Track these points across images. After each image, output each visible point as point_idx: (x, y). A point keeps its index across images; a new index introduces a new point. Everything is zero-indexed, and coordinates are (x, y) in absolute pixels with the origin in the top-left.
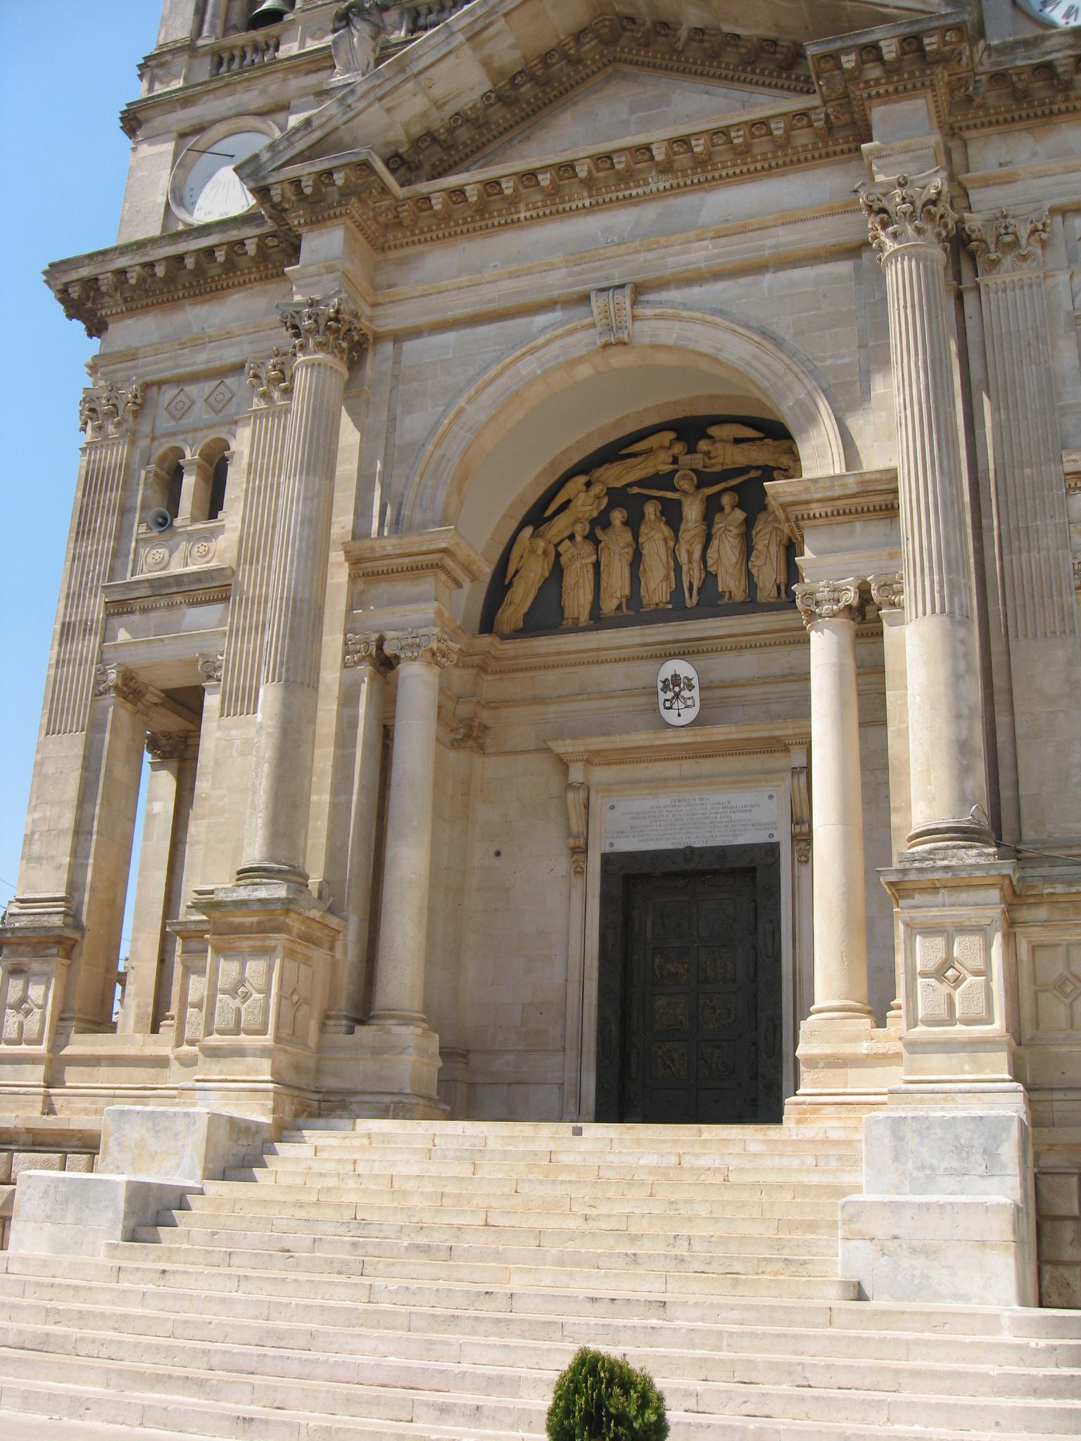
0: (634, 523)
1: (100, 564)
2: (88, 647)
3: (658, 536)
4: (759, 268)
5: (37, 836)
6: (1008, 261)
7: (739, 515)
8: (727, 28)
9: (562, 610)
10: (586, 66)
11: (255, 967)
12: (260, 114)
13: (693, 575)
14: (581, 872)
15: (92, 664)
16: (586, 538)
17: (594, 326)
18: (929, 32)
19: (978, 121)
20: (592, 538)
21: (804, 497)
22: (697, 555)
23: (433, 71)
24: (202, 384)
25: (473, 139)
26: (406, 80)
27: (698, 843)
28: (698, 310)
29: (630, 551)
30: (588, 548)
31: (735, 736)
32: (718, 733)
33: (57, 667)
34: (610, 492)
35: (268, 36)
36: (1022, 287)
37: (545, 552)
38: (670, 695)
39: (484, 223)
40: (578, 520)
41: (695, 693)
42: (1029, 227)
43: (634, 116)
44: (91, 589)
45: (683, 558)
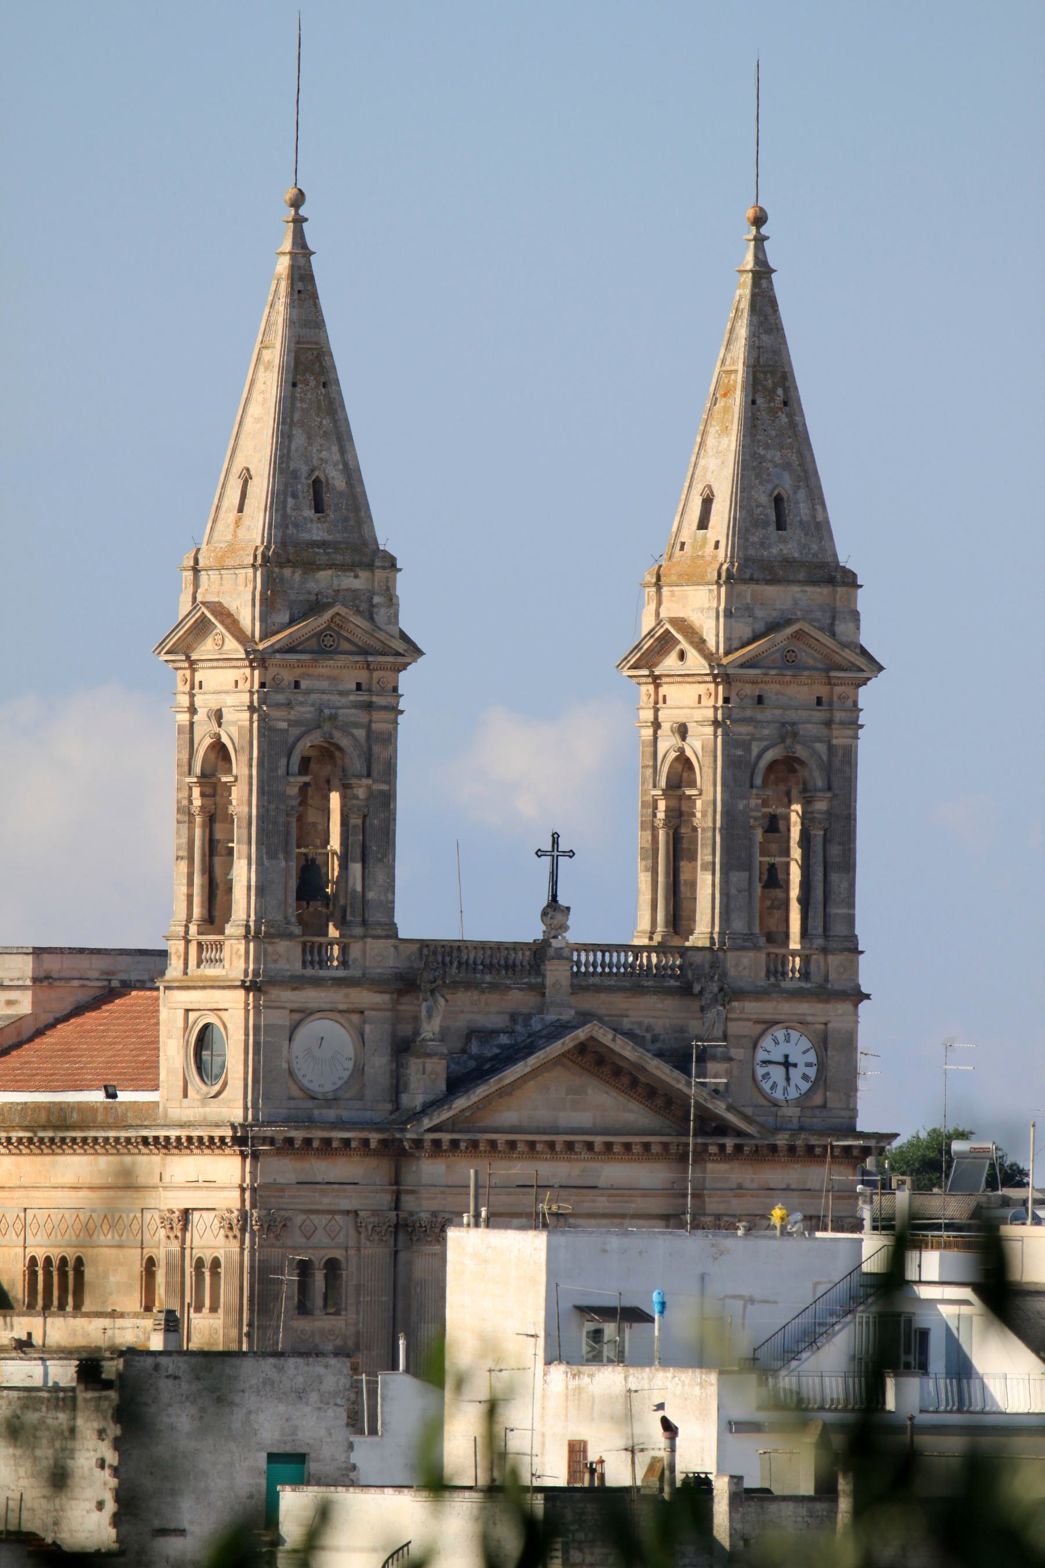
12: (340, 1012)
24: (320, 1216)
43: (569, 1097)
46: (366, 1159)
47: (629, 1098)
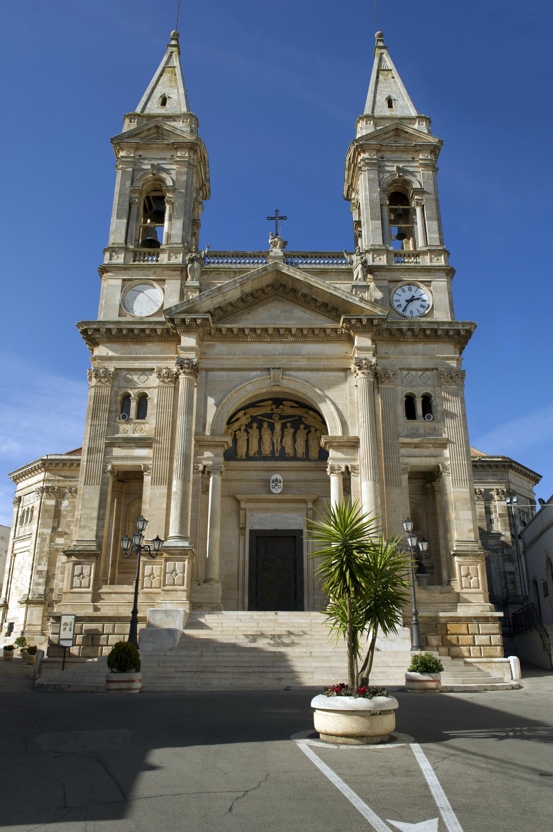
0: (260, 428)
1: (102, 429)
2: (99, 457)
3: (268, 433)
4: (318, 370)
5: (82, 519)
6: (387, 381)
7: (292, 430)
8: (313, 296)
9: (237, 453)
10: (268, 295)
11: (179, 565)
13: (278, 447)
14: (244, 535)
15: (101, 463)
16: (244, 431)
17: (270, 378)
18: (376, 319)
19: (381, 339)
20: (246, 430)
21: (333, 441)
22: (279, 441)
23: (229, 292)
25: (232, 311)
26: (221, 294)
27: (279, 528)
28: (301, 380)
29: (258, 437)
30: (245, 434)
31: (292, 498)
32: (288, 497)
33: (87, 462)
34: (252, 417)
35: (155, 251)
36: (390, 389)
37: (231, 433)
38: (274, 484)
39: (236, 339)
40: (241, 425)
41: (282, 484)
42: (393, 373)
44: (99, 437)
45: (275, 441)
46: (162, 344)
47: (317, 314)
